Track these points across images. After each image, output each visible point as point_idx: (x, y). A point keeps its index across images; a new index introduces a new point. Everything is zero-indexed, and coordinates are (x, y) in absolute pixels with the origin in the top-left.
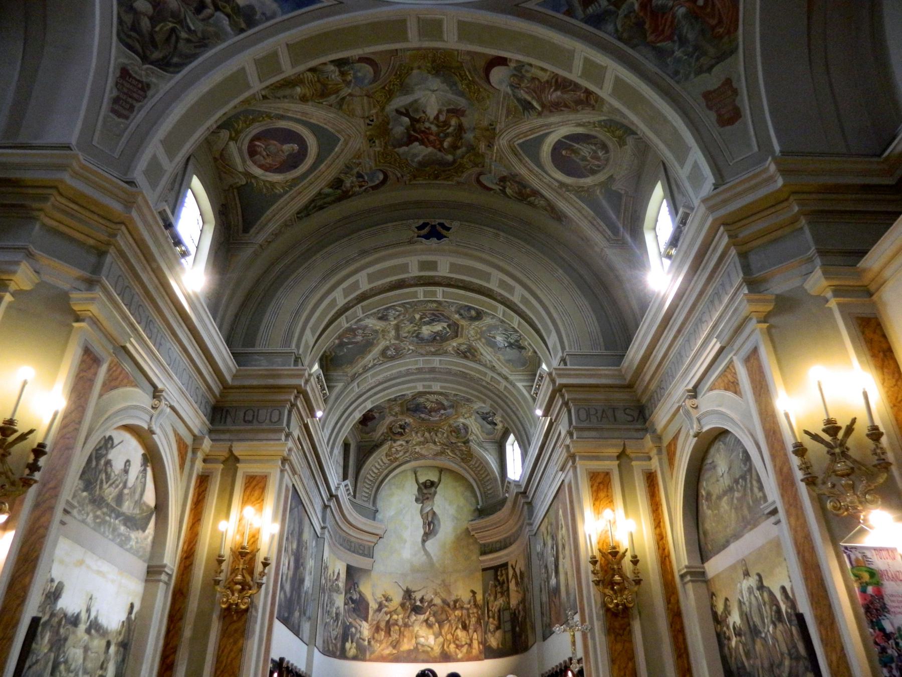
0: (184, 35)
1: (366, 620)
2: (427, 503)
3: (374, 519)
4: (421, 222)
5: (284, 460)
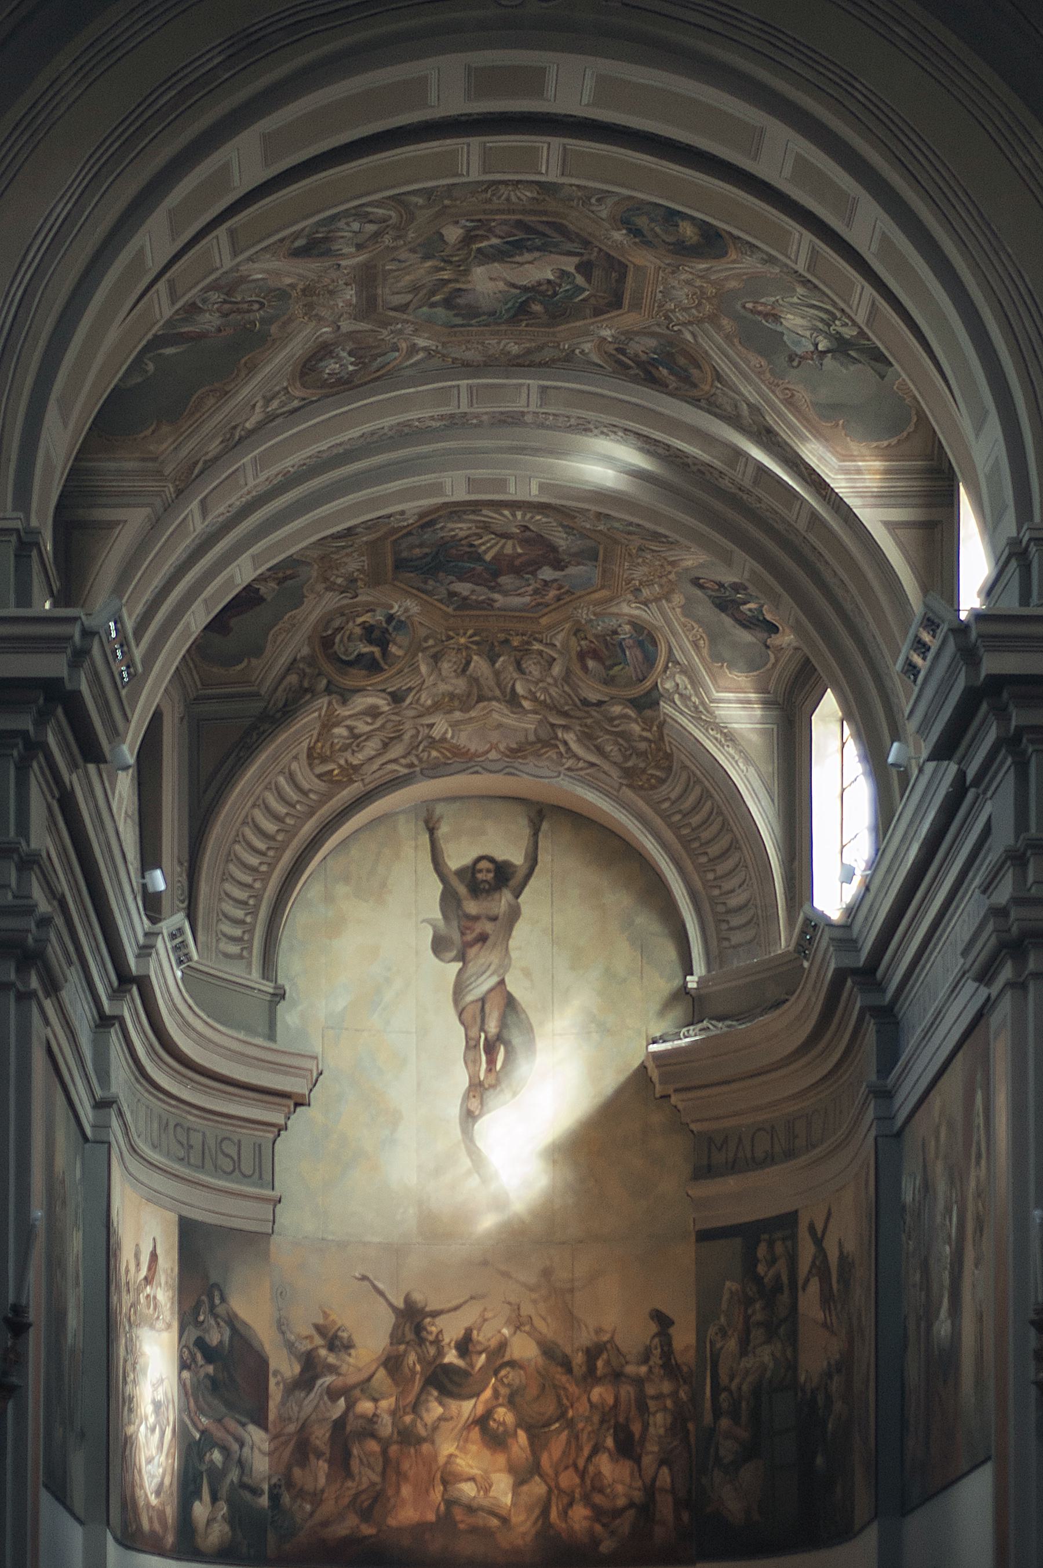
2: (484, 958)
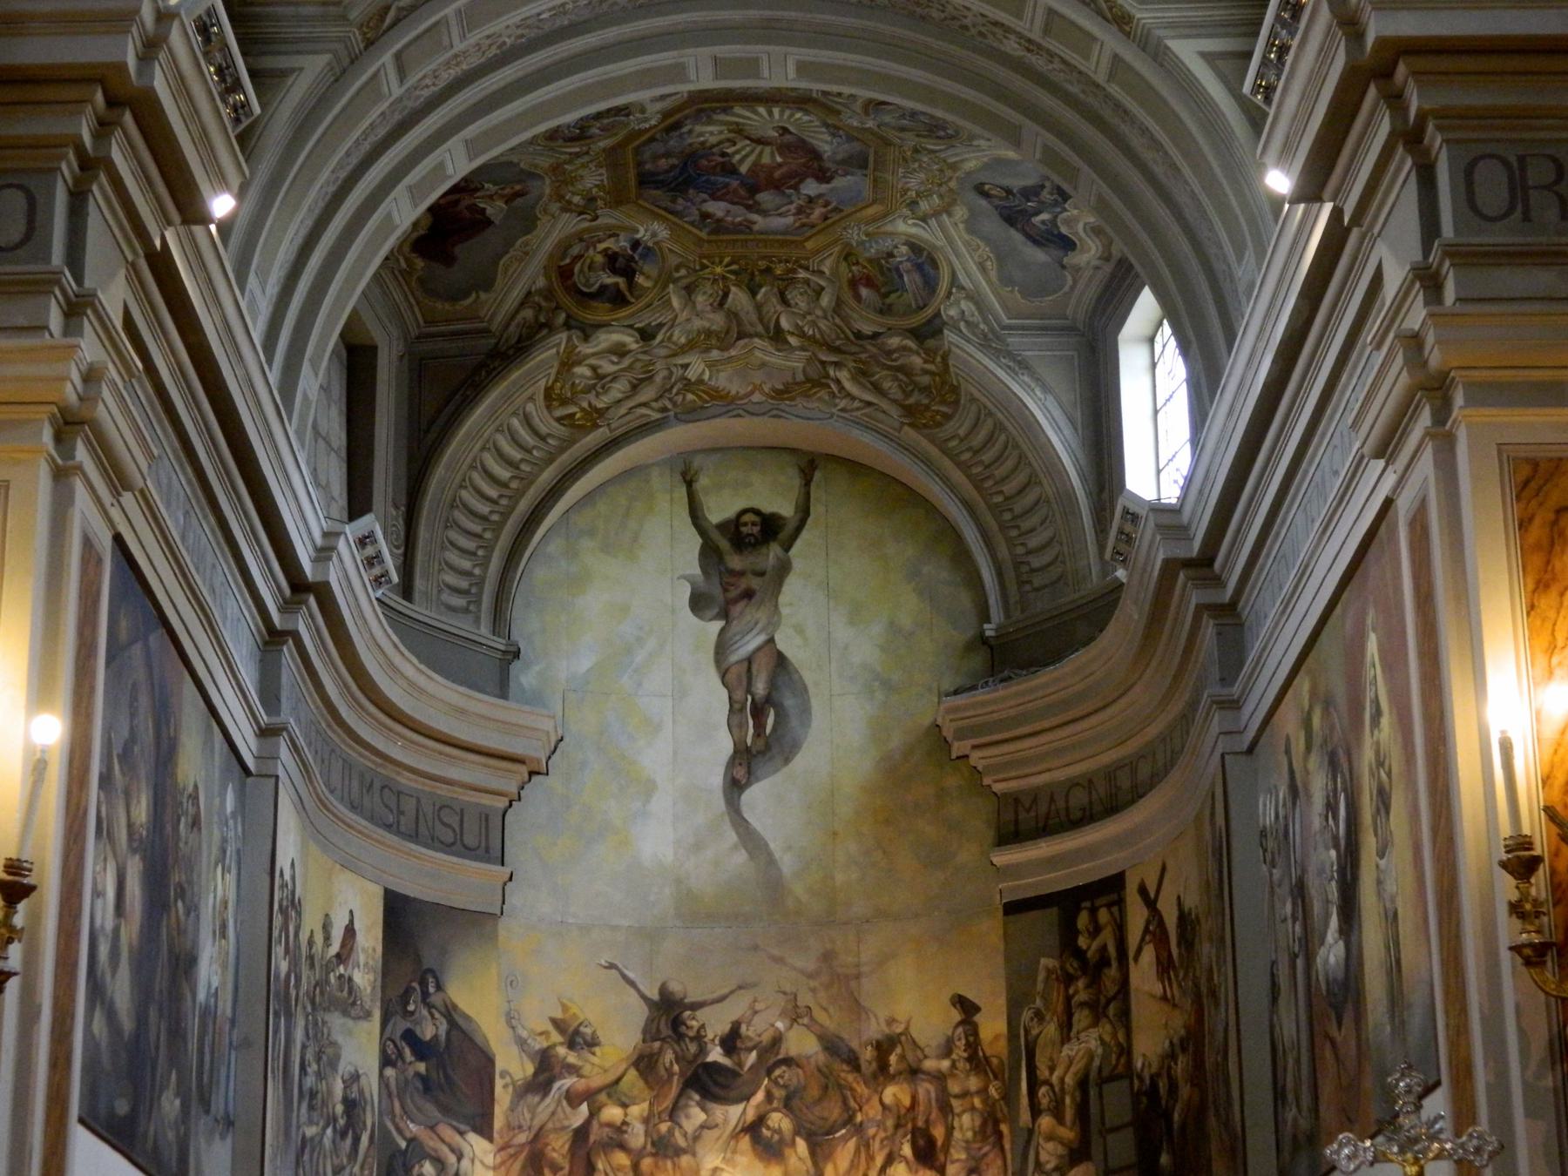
1: (484, 1128)
3: (502, 689)
5: (68, 425)
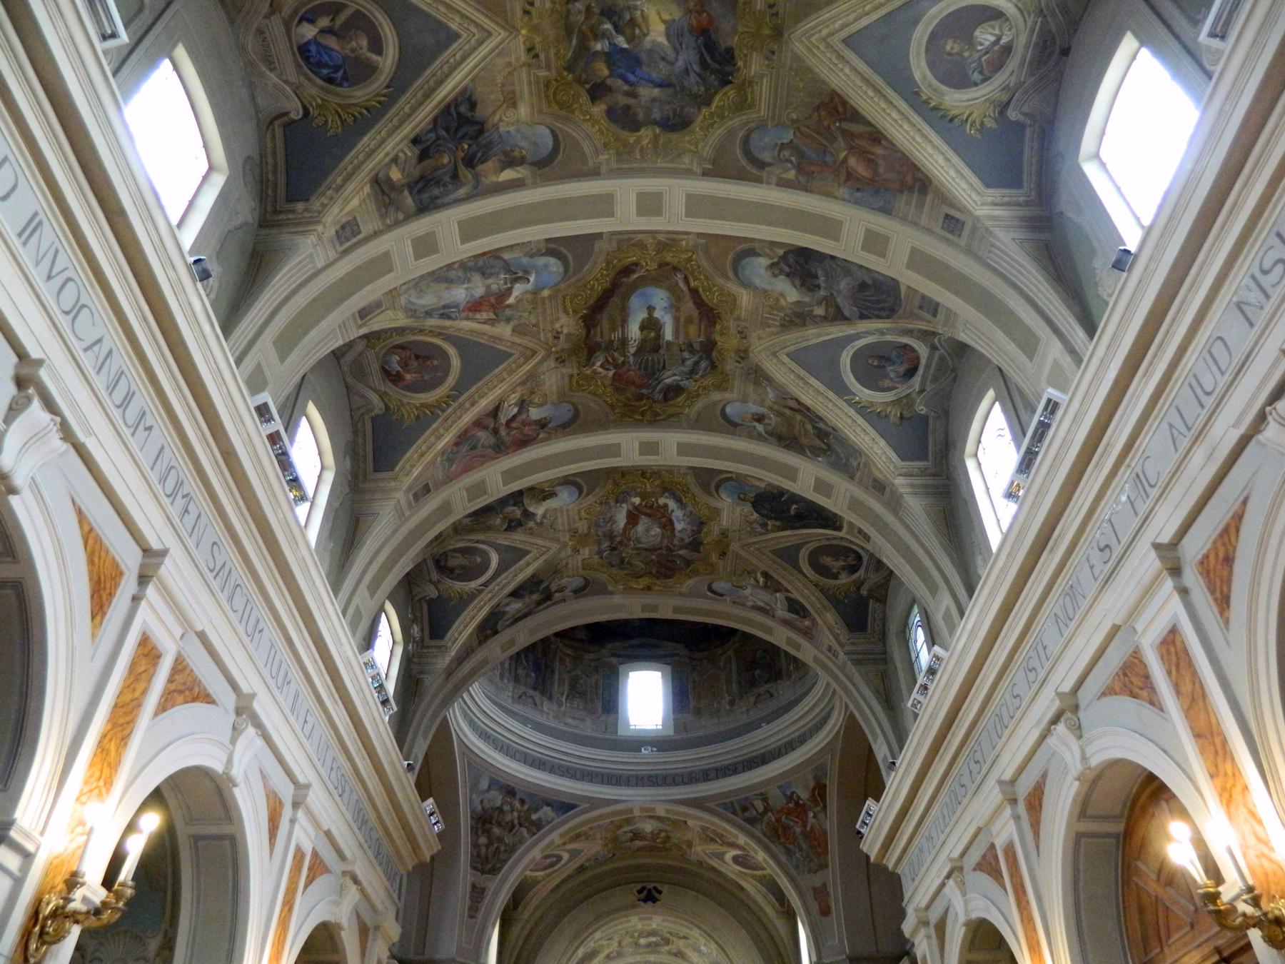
0: (503, 848)
4: (639, 886)
